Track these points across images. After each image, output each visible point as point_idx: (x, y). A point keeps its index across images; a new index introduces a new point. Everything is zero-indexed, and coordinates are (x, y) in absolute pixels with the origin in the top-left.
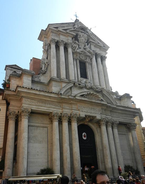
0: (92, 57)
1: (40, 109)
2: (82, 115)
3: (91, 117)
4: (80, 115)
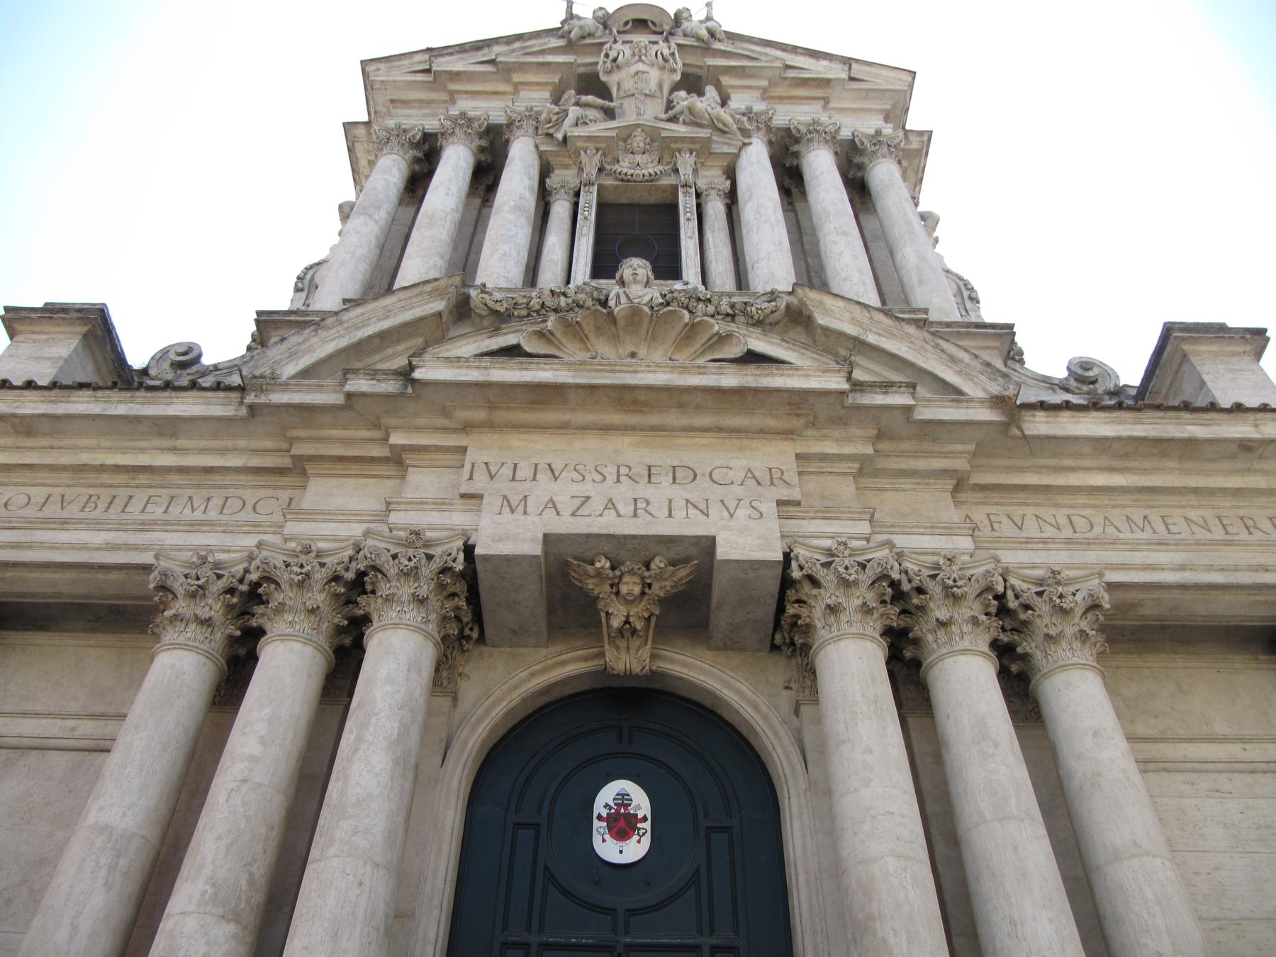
1: (42, 546)
4: (469, 550)
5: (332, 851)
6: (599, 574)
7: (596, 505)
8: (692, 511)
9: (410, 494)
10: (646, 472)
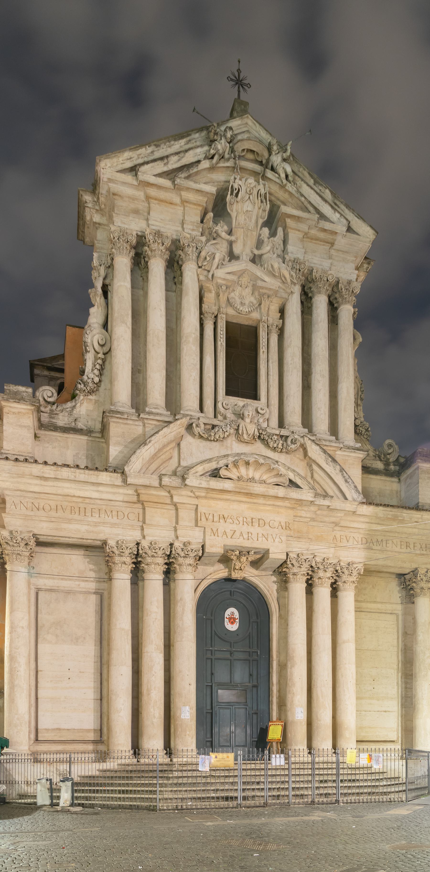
7: (237, 534)
8: (264, 538)
10: (251, 521)
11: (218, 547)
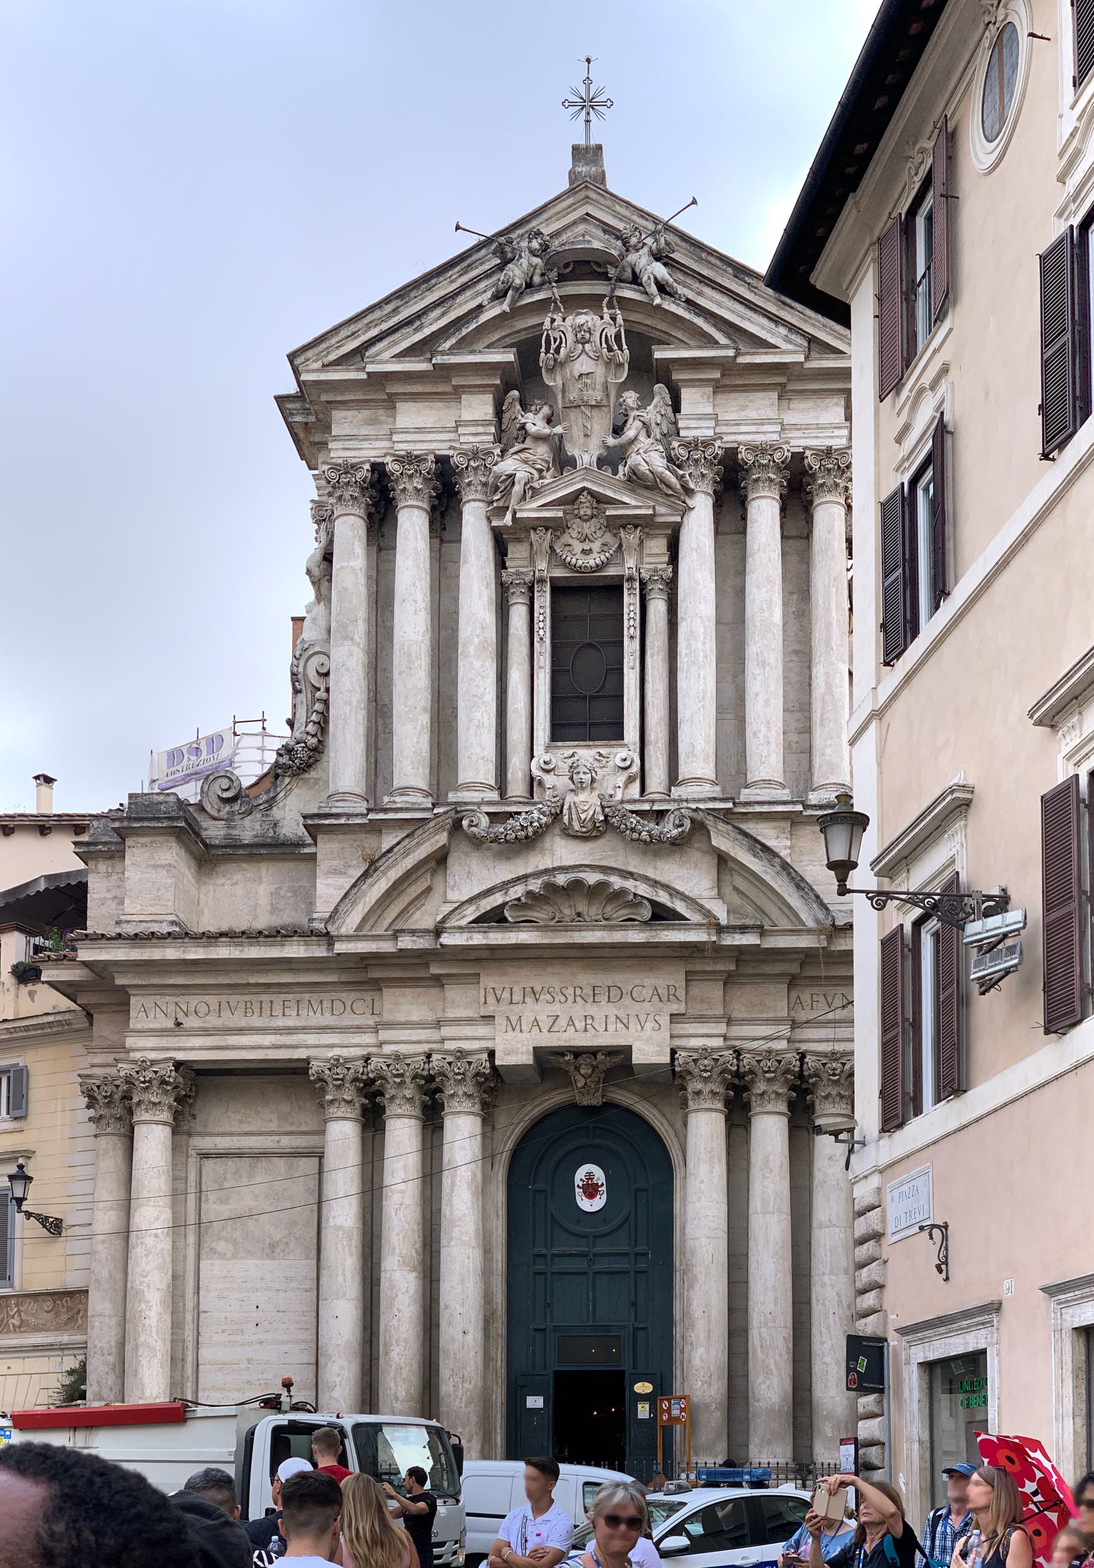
0: (678, 519)
2: (508, 1053)
3: (600, 1057)
4: (492, 1054)
5: (453, 1243)
6: (567, 1062)
7: (563, 1022)
8: (620, 1025)
9: (451, 1014)
11: (522, 1053)
